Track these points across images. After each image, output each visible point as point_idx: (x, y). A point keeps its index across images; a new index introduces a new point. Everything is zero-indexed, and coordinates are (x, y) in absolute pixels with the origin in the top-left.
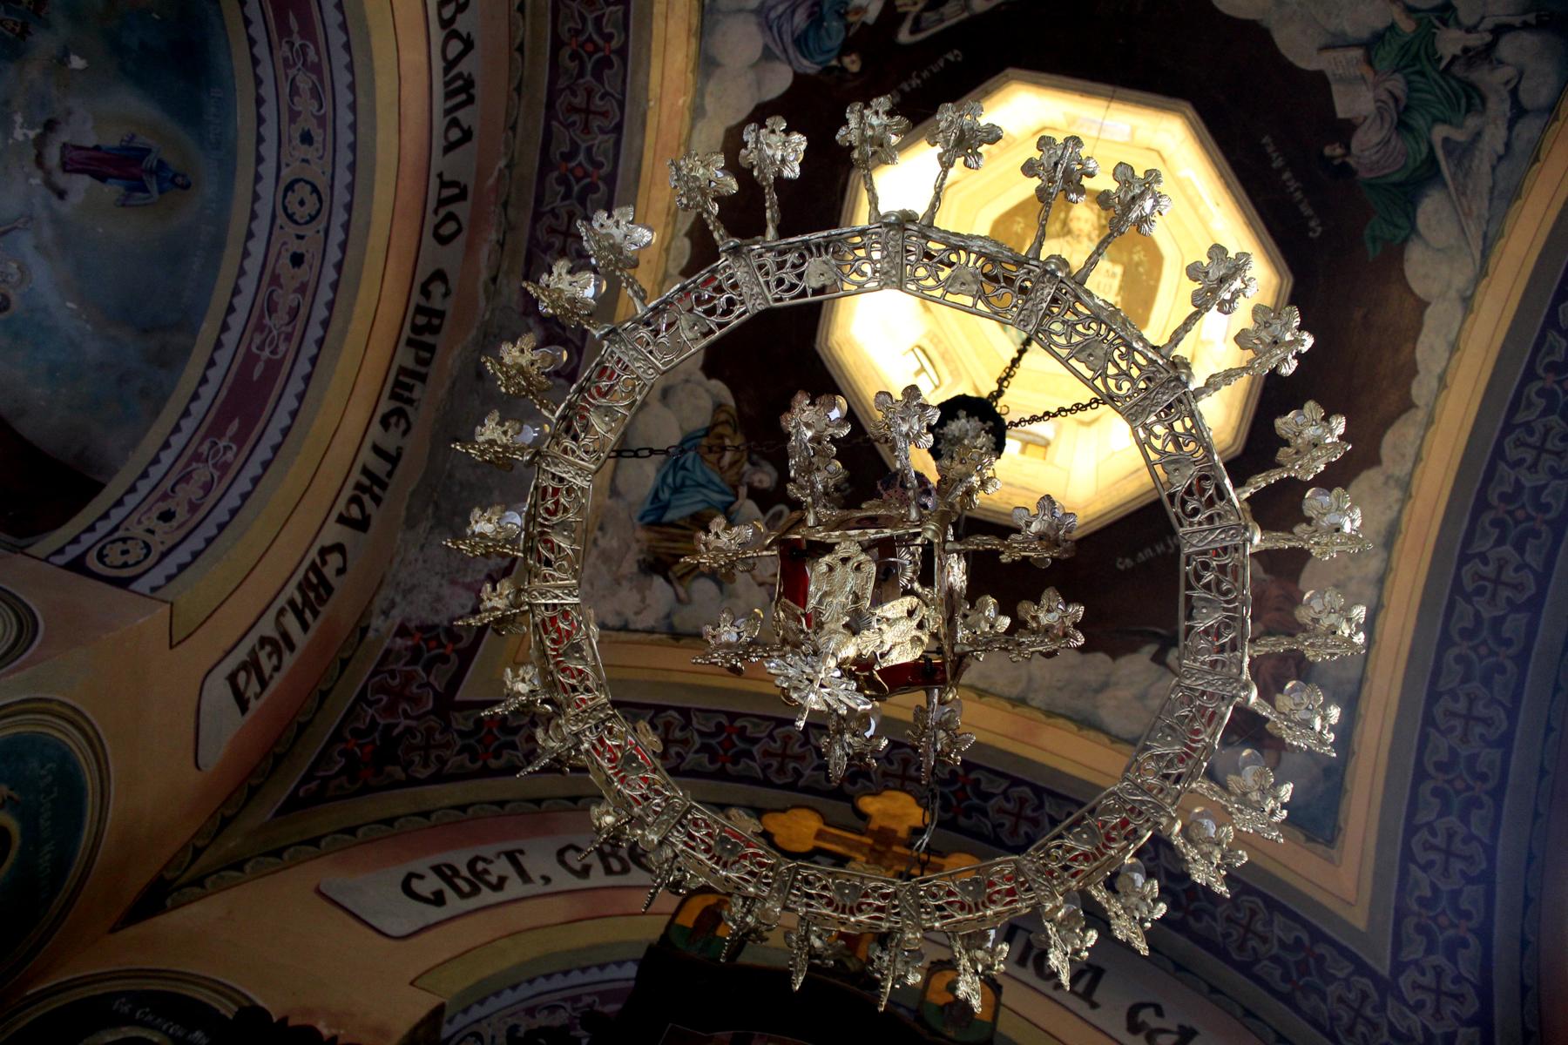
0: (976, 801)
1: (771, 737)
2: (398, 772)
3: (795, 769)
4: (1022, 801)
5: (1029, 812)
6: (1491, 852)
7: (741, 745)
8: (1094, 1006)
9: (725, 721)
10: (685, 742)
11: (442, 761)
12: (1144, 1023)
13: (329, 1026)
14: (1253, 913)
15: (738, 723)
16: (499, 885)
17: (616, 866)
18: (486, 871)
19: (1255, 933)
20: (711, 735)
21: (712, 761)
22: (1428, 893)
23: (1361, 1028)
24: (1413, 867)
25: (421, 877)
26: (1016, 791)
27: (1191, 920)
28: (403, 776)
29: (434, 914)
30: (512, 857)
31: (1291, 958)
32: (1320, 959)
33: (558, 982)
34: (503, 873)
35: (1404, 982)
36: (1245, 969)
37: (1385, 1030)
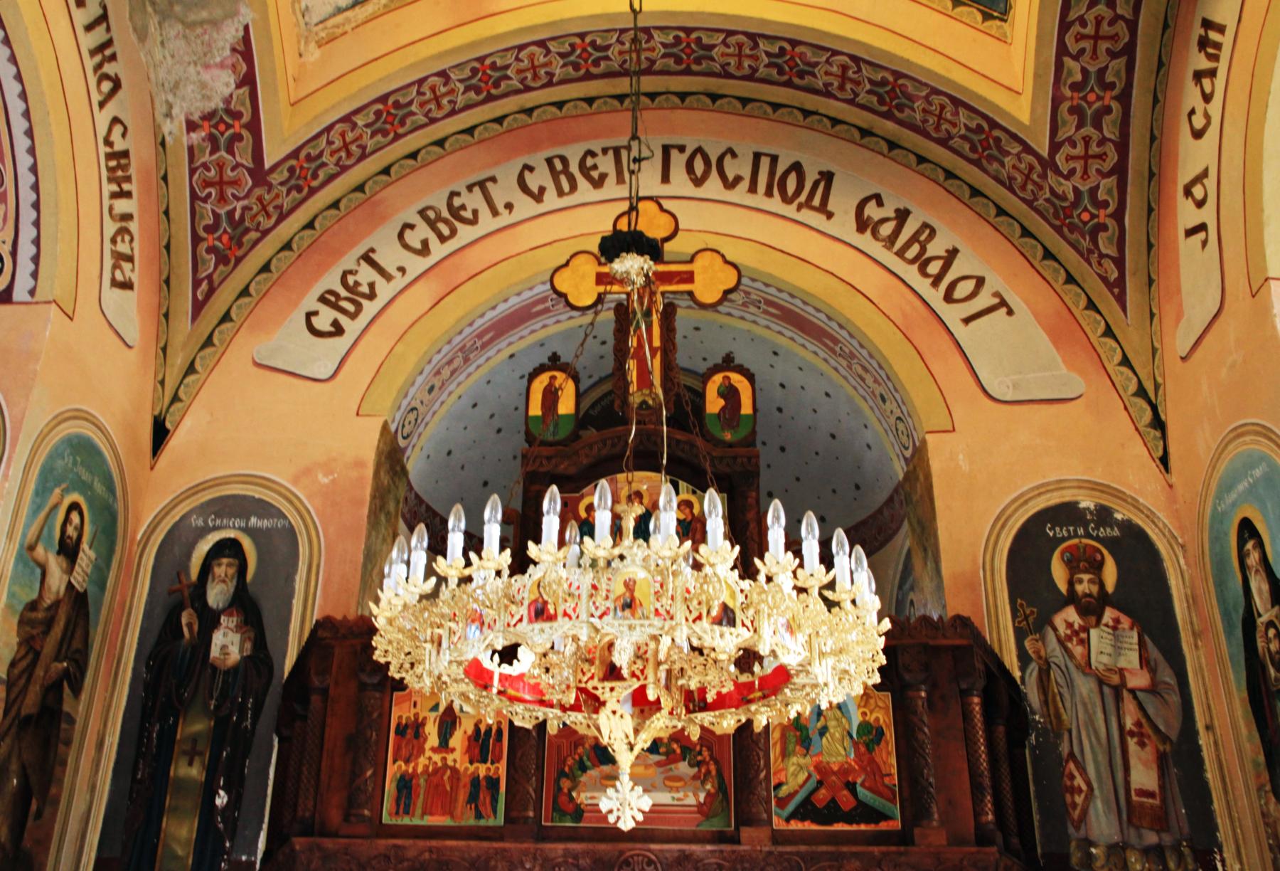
0: (702, 52)
1: (517, 59)
2: (254, 235)
3: (547, 73)
4: (740, 46)
5: (748, 51)
6: (1132, 26)
7: (497, 74)
8: (830, 215)
9: (477, 65)
10: (452, 92)
11: (279, 207)
12: (869, 218)
13: (326, 475)
14: (943, 107)
15: (488, 62)
16: (371, 296)
17: (445, 231)
18: (357, 284)
19: (946, 120)
20: (470, 78)
21: (478, 93)
22: (1078, 77)
23: (1030, 187)
24: (1067, 60)
25: (316, 313)
26: (732, 40)
27: (896, 112)
28: (258, 235)
29: (340, 345)
30: (367, 258)
31: (975, 138)
32: (997, 140)
33: (446, 349)
34: (370, 280)
35: (1060, 159)
36: (943, 143)
37: (1047, 190)
